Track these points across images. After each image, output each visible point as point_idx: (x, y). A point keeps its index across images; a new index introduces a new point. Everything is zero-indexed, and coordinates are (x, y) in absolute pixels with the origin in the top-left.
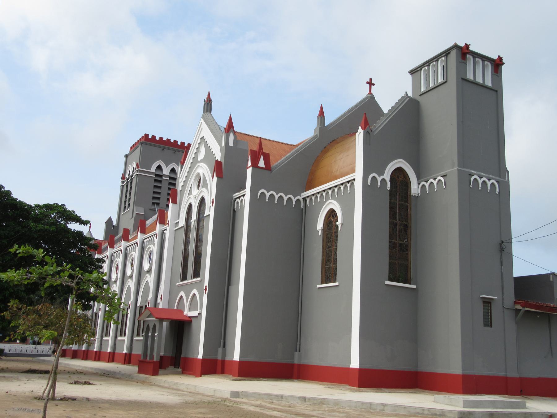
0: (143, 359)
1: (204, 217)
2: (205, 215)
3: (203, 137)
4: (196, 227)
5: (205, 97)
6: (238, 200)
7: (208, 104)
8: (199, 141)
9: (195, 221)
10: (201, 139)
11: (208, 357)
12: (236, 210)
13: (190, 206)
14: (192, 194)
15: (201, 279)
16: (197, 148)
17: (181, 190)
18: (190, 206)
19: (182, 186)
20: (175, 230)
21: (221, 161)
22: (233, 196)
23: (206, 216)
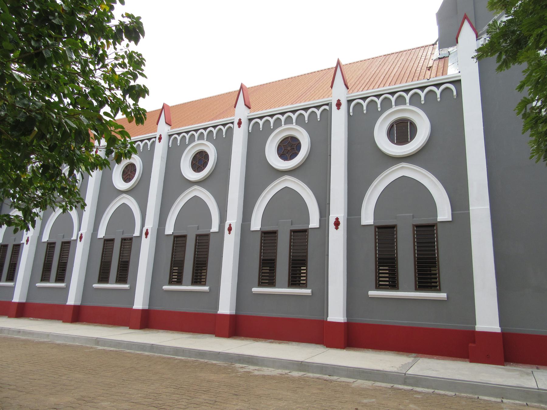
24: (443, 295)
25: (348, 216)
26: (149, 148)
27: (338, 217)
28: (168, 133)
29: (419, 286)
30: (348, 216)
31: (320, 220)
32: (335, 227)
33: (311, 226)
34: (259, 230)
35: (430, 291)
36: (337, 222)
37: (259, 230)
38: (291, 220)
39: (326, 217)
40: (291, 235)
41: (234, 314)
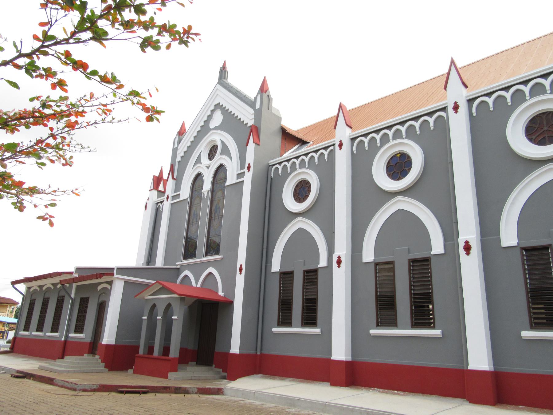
0: (144, 353)
1: (225, 187)
2: (226, 184)
3: (219, 103)
4: (210, 199)
5: (221, 65)
6: (278, 166)
7: (223, 72)
8: (212, 108)
9: (208, 191)
10: (215, 106)
11: (245, 352)
12: (272, 177)
13: (198, 177)
14: (200, 163)
15: (222, 257)
16: (208, 116)
17: (179, 162)
18: (198, 177)
19: (182, 157)
20: (172, 204)
21: (255, 125)
22: (269, 162)
23: (227, 186)
24: (437, 332)
25: (481, 237)
26: (161, 209)
27: (468, 240)
28: (155, 202)
29: (415, 323)
30: (352, 253)
31: (445, 245)
32: (466, 253)
33: (434, 252)
34: (278, 271)
35: (306, 327)
36: (339, 260)
37: (278, 271)
38: (303, 260)
39: (454, 240)
40: (410, 266)
41: (114, 343)
